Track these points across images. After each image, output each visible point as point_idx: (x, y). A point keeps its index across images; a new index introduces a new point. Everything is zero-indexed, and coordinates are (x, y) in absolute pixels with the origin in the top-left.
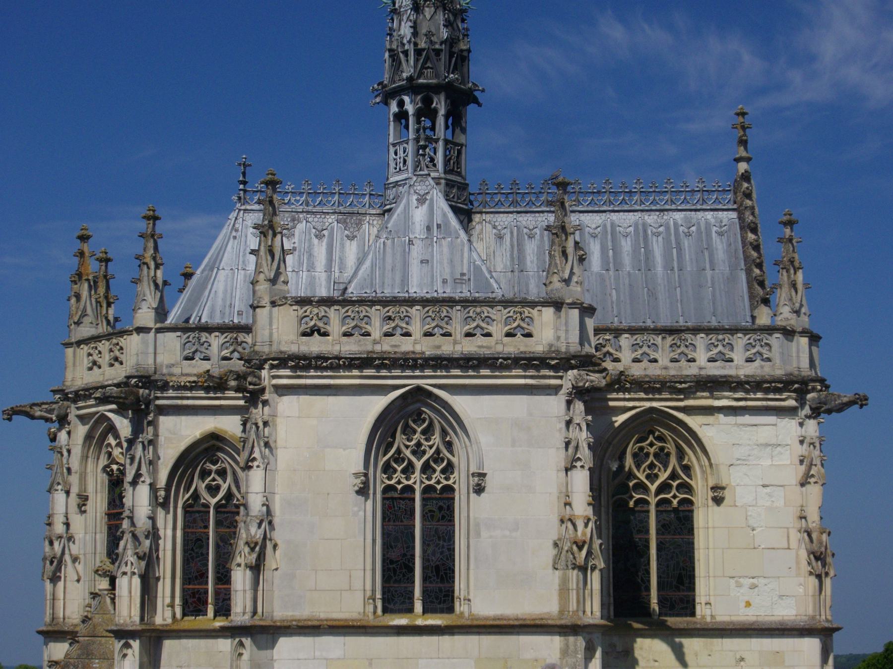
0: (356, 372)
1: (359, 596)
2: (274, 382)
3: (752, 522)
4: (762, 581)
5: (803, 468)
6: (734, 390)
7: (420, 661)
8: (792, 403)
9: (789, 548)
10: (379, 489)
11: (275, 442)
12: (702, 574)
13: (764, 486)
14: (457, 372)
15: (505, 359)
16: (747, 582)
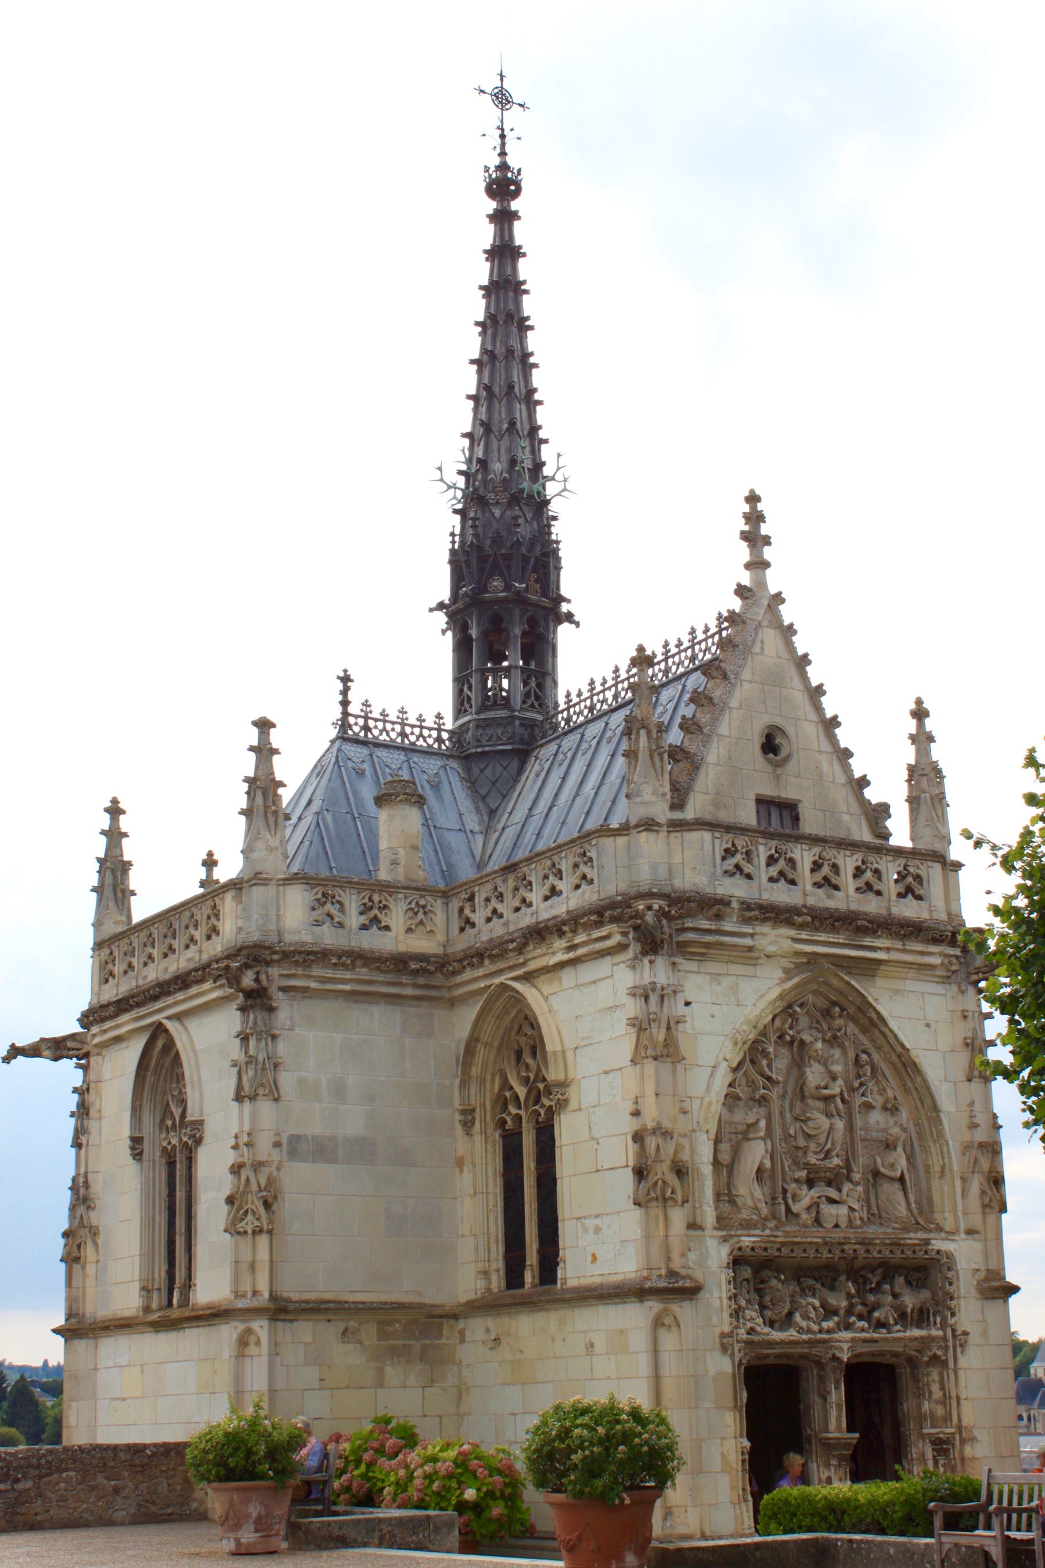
0: (125, 1017)
1: (136, 1287)
2: (97, 1040)
3: (596, 1134)
4: (606, 1220)
5: (634, 1036)
6: (561, 934)
7: (169, 1366)
8: (617, 938)
9: (627, 1166)
10: (158, 1154)
11: (100, 1111)
12: (567, 1215)
13: (606, 1072)
14: (180, 996)
15: (196, 970)
16: (590, 1223)
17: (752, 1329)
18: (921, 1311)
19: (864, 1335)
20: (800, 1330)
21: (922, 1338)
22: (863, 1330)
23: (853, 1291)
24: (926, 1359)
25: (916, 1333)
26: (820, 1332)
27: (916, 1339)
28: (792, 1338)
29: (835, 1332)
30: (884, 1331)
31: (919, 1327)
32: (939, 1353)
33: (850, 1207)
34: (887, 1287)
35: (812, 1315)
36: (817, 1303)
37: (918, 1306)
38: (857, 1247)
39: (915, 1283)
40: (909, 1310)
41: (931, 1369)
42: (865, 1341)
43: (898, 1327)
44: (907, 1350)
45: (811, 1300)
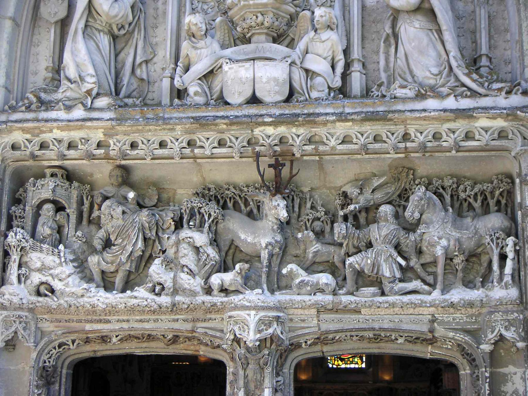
17: (42, 283)
18: (472, 257)
19: (319, 297)
20: (158, 289)
21: (471, 304)
22: (319, 289)
23: (283, 214)
24: (486, 347)
25: (458, 294)
26: (209, 291)
27: (452, 305)
28: (135, 301)
29: (237, 292)
30: (372, 290)
31: (468, 284)
32: (509, 335)
33: (307, 71)
34: (386, 209)
35: (188, 258)
36: (201, 238)
37: (469, 245)
38: (282, 130)
39: (477, 205)
40: (439, 252)
41: (511, 369)
42: (321, 309)
43: (416, 284)
44: (440, 331)
45: (186, 233)
